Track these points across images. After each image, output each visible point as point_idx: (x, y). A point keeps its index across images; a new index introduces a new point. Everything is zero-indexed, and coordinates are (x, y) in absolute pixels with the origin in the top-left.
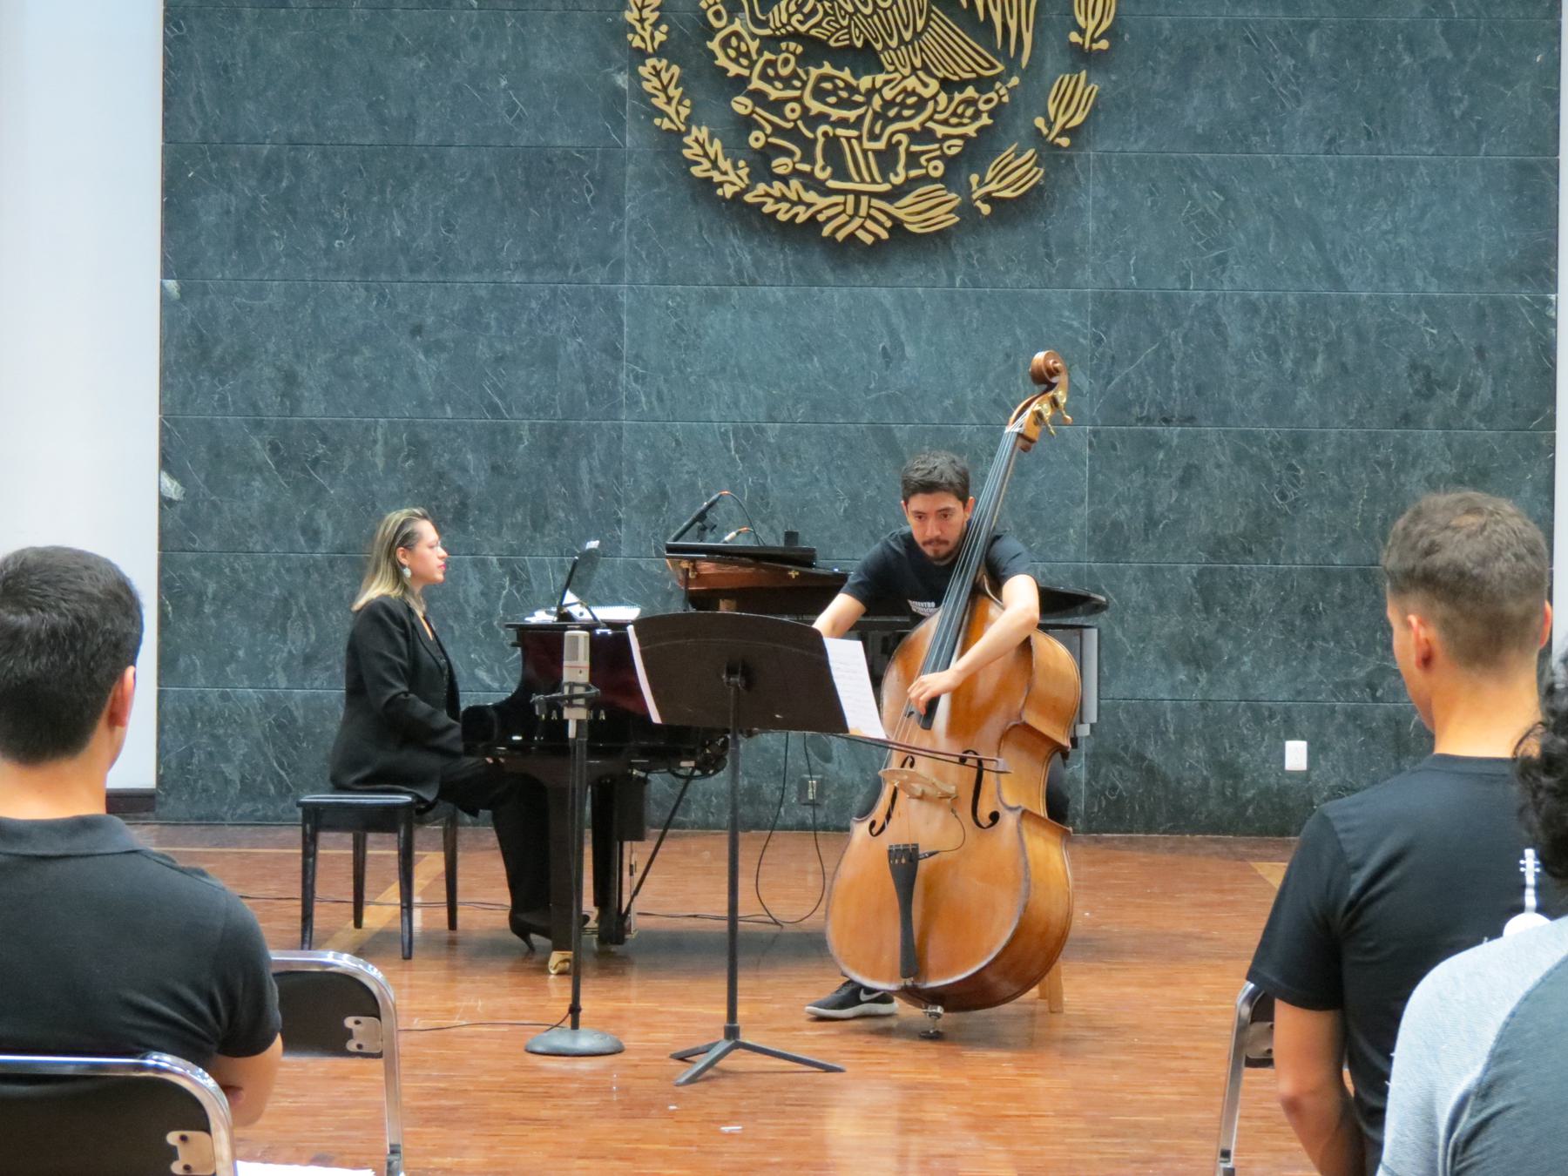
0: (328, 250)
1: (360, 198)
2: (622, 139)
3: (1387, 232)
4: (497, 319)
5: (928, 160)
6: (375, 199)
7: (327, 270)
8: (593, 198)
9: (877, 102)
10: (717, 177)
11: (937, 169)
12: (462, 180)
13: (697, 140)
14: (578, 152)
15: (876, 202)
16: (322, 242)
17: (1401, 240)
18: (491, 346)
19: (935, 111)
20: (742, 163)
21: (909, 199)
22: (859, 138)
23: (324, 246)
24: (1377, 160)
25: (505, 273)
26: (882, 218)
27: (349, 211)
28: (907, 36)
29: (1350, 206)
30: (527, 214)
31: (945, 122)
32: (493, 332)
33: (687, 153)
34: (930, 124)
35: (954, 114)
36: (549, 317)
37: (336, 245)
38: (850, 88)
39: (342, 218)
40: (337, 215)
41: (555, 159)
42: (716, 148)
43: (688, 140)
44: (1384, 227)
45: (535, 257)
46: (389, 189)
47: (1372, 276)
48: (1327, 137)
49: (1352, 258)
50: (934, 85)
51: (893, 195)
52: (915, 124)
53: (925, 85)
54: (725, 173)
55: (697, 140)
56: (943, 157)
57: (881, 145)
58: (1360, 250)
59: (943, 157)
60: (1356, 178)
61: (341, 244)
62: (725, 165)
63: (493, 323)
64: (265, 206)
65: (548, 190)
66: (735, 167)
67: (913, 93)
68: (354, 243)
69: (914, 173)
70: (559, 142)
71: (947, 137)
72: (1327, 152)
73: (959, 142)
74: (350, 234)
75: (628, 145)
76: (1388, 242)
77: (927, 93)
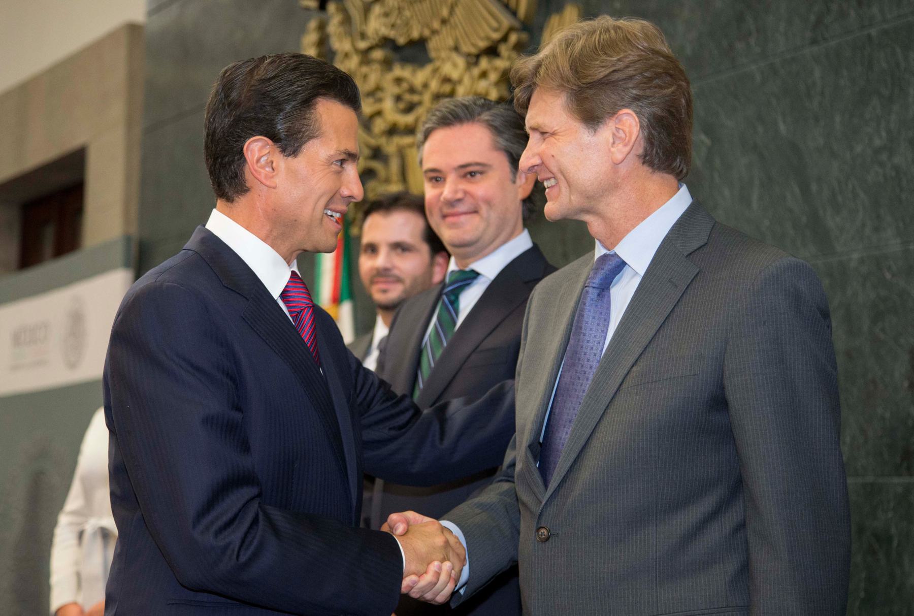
3: (877, 151)
17: (897, 160)
24: (869, 37)
28: (445, 12)
29: (838, 119)
38: (412, 90)
44: (877, 142)
47: (864, 225)
48: (813, 18)
49: (840, 199)
50: (461, 62)
53: (455, 65)
58: (850, 186)
60: (845, 73)
67: (447, 80)
72: (814, 42)
76: (882, 164)
77: (455, 75)
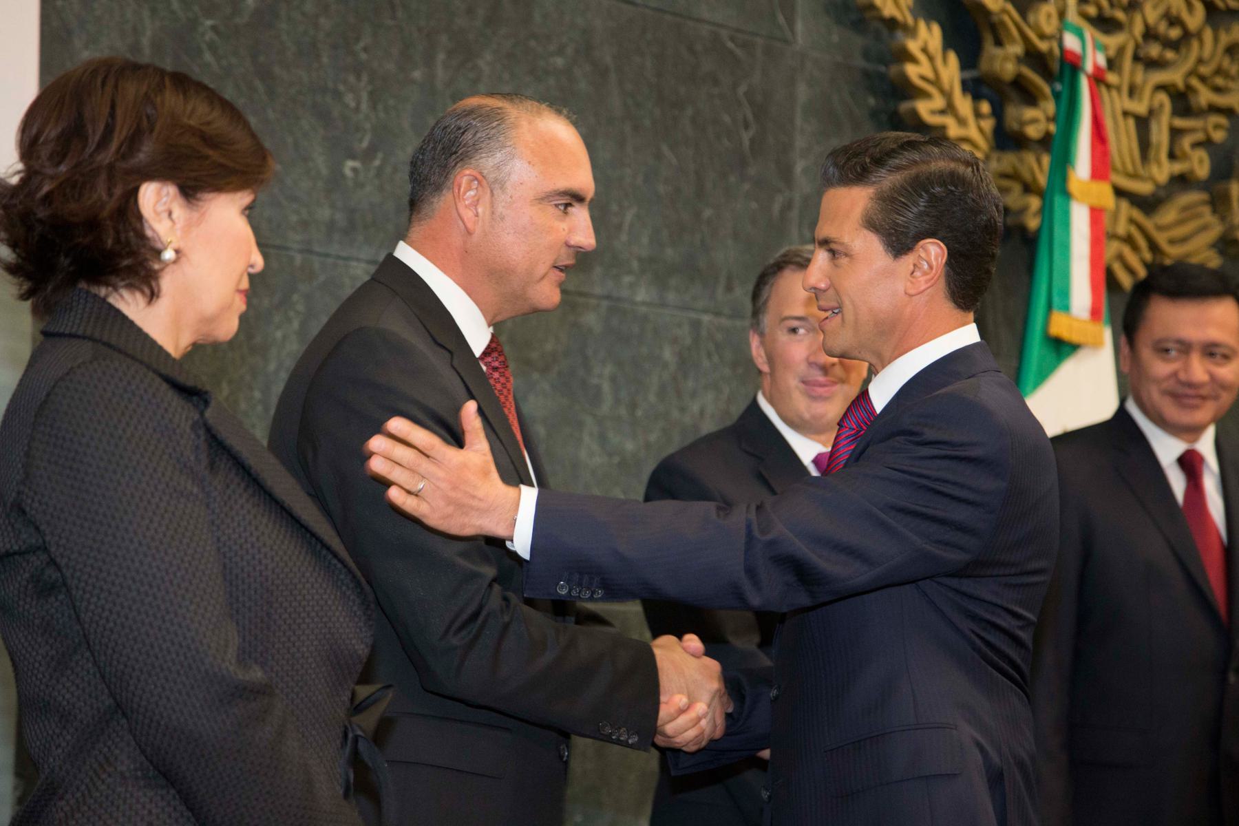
0: (336, 179)
1: (390, 66)
2: (791, 22)
4: (613, 379)
5: (1196, 145)
6: (417, 74)
7: (331, 226)
8: (752, 141)
9: (1138, 29)
10: (954, 131)
11: (1200, 164)
12: (559, 62)
13: (925, 50)
14: (732, 39)
15: (1137, 214)
16: (321, 162)
18: (602, 439)
19: (1200, 61)
20: (985, 107)
21: (1169, 215)
22: (1119, 89)
23: (325, 172)
25: (627, 279)
26: (1142, 242)
27: (371, 94)
30: (659, 156)
31: (1203, 79)
32: (605, 407)
33: (912, 71)
34: (1195, 82)
35: (1219, 71)
36: (690, 384)
37: (348, 172)
39: (357, 109)
40: (349, 99)
41: (699, 47)
42: (951, 71)
43: (913, 46)
45: (669, 253)
46: (441, 56)
51: (1148, 204)
52: (1175, 76)
54: (962, 122)
55: (925, 50)
56: (1207, 143)
57: (1141, 108)
59: (1207, 143)
61: (354, 170)
62: (964, 105)
63: (606, 387)
64: (212, 47)
65: (689, 112)
66: (978, 115)
68: (379, 172)
69: (1178, 168)
70: (706, 15)
71: (1214, 109)
73: (1222, 120)
74: (368, 155)
75: (800, 40)
